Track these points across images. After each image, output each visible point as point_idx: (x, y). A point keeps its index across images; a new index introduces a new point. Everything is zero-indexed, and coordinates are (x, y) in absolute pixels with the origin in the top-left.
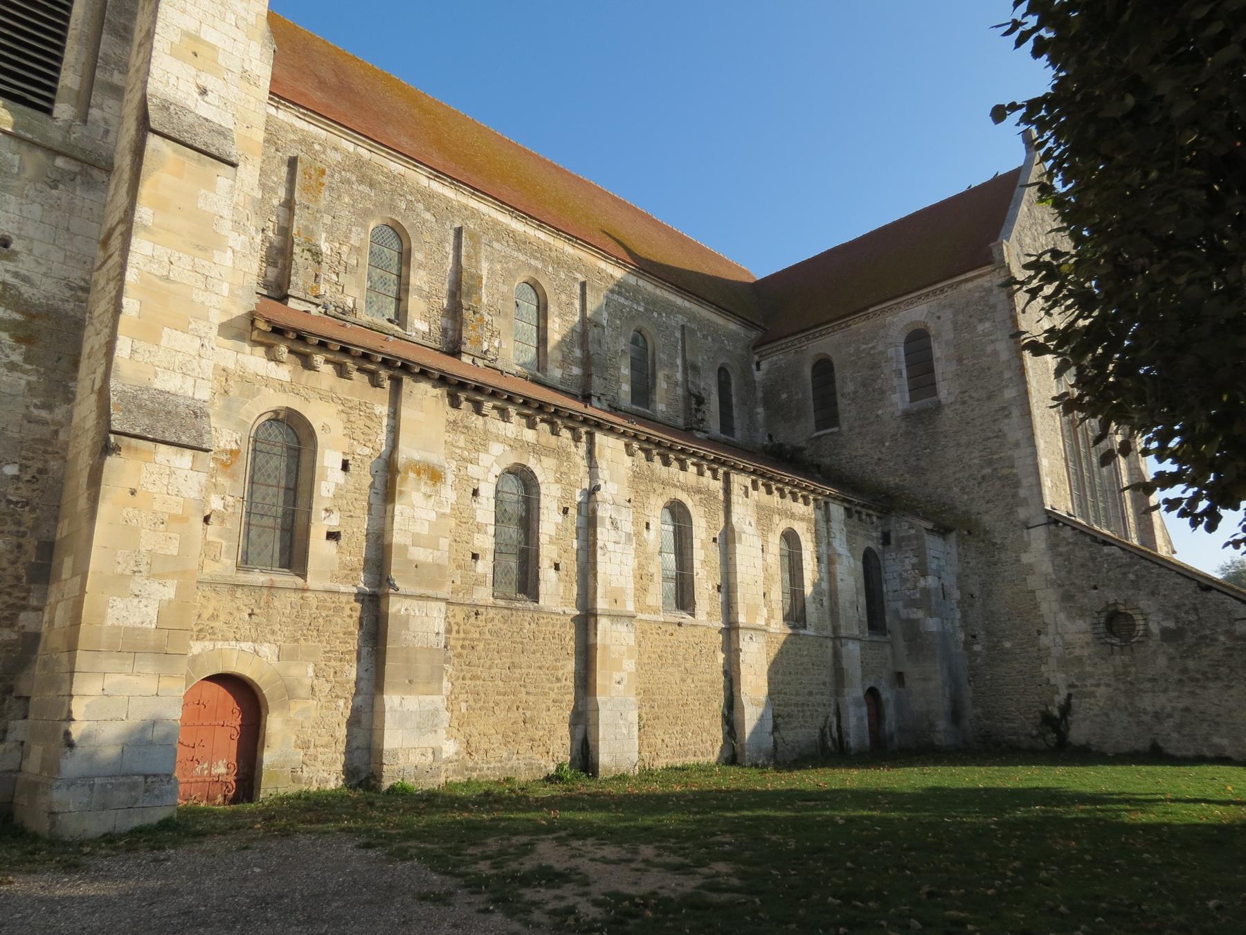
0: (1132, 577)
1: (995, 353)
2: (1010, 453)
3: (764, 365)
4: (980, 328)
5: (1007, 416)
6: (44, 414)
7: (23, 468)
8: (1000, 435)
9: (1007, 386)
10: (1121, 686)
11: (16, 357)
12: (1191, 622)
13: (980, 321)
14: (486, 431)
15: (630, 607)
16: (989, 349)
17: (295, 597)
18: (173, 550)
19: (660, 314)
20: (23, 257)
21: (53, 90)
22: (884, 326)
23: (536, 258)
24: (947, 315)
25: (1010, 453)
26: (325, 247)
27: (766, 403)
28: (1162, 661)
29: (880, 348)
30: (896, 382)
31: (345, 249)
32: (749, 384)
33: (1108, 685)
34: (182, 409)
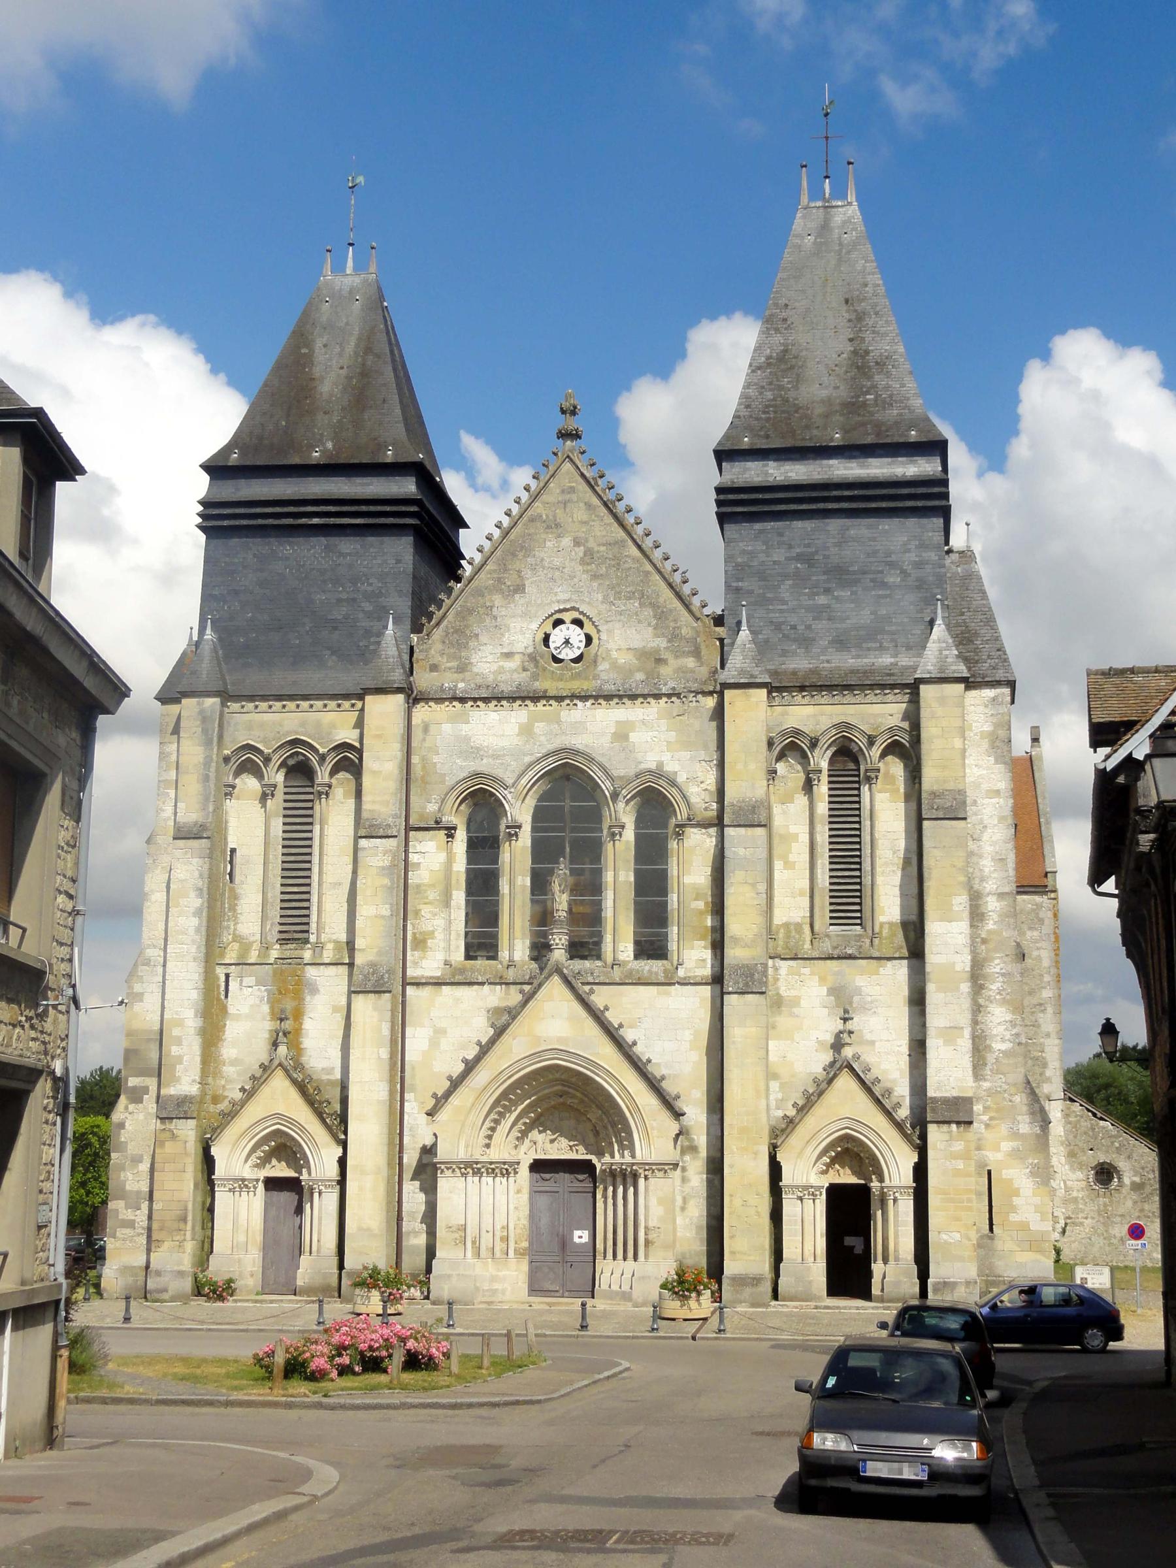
0: (1117, 1145)
1: (1039, 958)
2: (1042, 1040)
4: (1029, 934)
5: (1044, 1011)
8: (1036, 1025)
9: (1045, 988)
10: (1101, 1219)
12: (1149, 1179)
13: (1030, 929)
16: (1035, 953)
25: (1042, 1040)
28: (1129, 1203)
33: (1093, 1218)
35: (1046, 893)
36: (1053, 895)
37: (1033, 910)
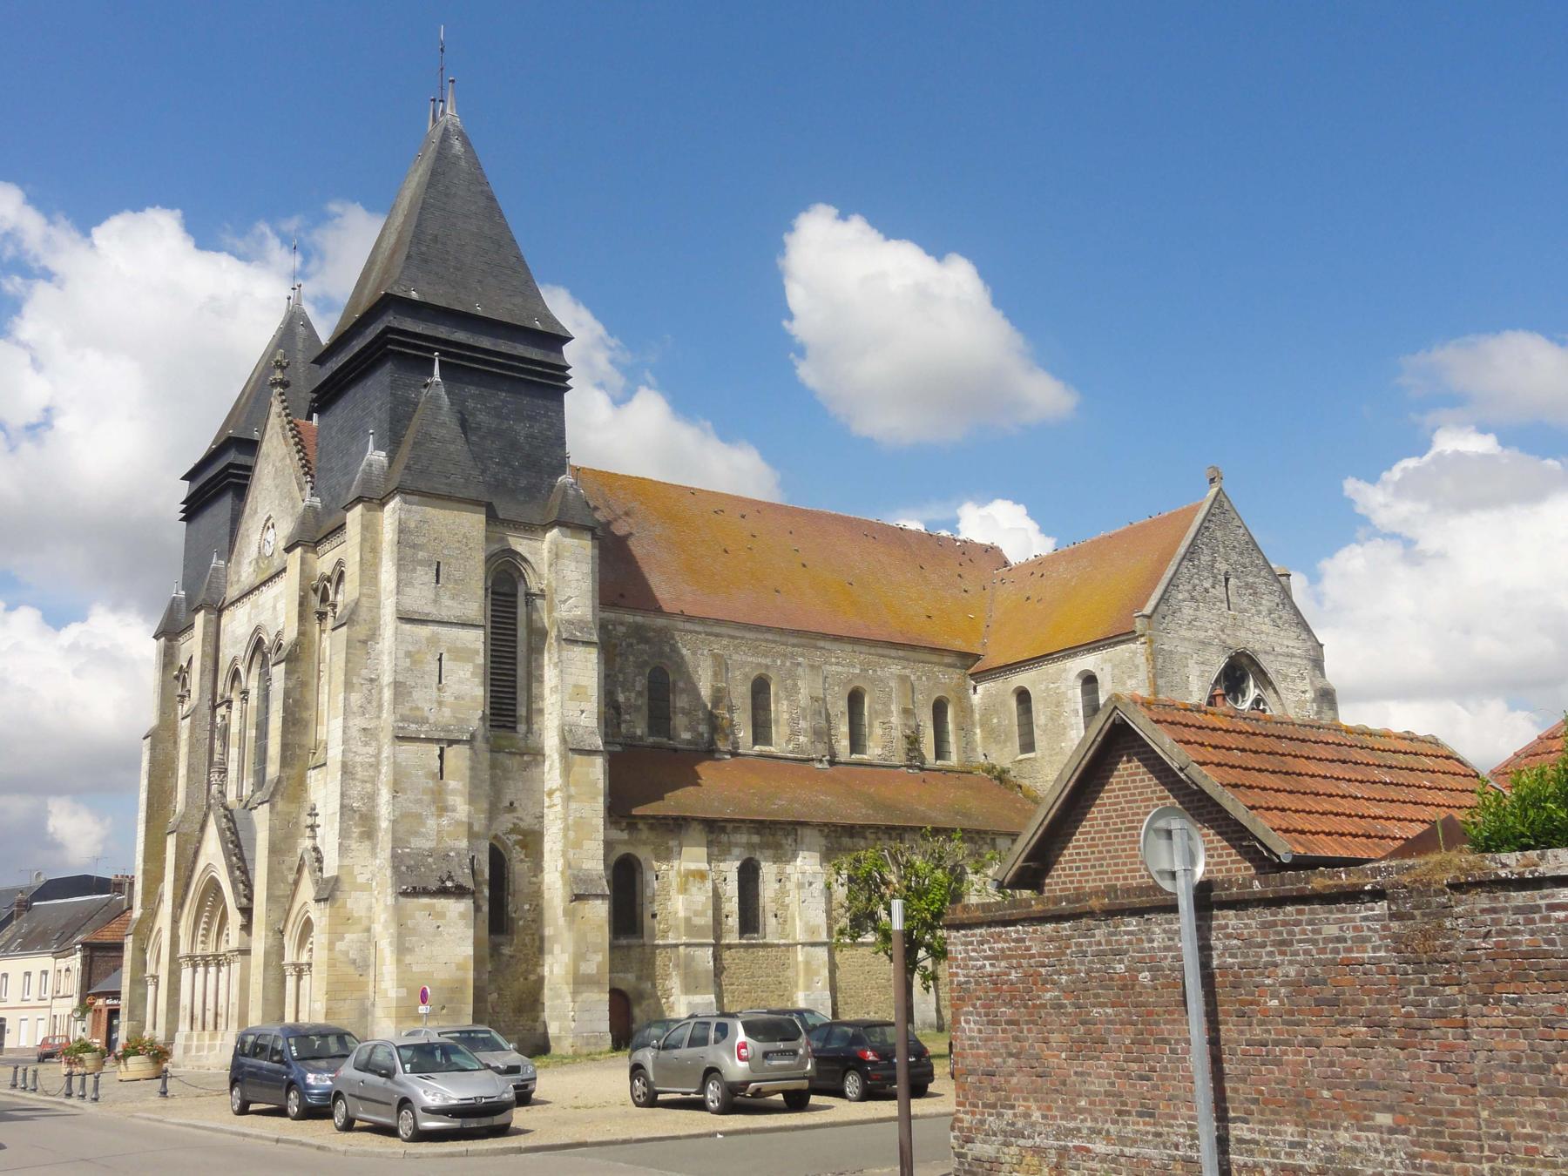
3: (980, 689)
6: (534, 879)
7: (531, 905)
11: (523, 857)
13: (1129, 677)
14: (729, 842)
15: (824, 938)
17: (640, 950)
18: (600, 940)
19: (875, 671)
20: (519, 809)
21: (514, 716)
22: (1065, 670)
23: (767, 657)
24: (1108, 668)
26: (621, 698)
27: (982, 726)
29: (1063, 689)
30: (1073, 720)
31: (633, 695)
32: (966, 710)
34: (596, 878)
35: (1136, 638)
36: (1143, 640)
37: (1131, 658)
